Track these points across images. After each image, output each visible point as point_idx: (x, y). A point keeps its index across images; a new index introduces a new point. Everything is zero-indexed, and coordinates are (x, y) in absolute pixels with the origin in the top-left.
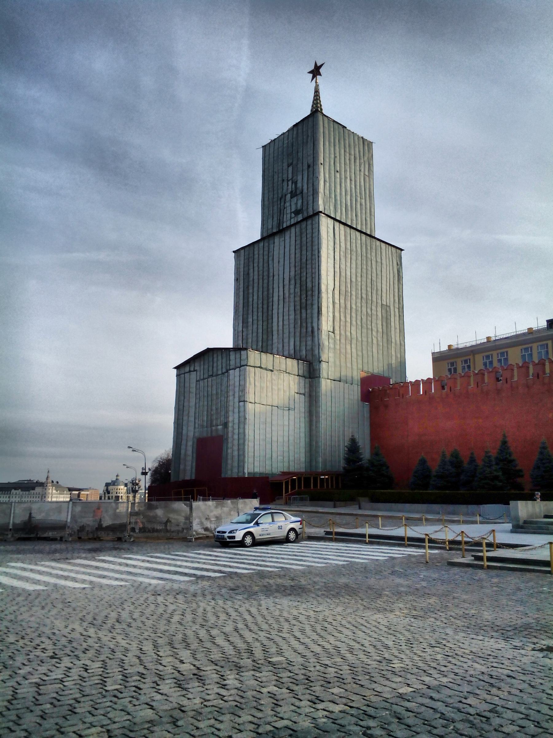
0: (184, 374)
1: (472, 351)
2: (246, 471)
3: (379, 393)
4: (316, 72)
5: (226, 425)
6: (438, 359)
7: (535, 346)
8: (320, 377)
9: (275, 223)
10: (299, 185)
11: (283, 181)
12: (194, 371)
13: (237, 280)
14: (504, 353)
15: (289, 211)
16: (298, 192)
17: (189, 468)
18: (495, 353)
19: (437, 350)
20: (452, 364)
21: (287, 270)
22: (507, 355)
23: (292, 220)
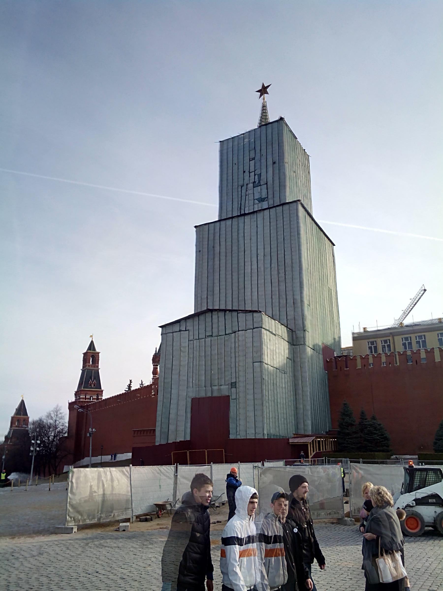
0: (173, 332)
1: (391, 333)
2: (265, 432)
3: (336, 363)
5: (233, 385)
6: (357, 338)
8: (305, 344)
9: (236, 205)
10: (263, 177)
11: (244, 172)
12: (186, 331)
13: (199, 252)
14: (422, 336)
15: (251, 197)
16: (262, 183)
17: (181, 428)
19: (356, 331)
20: (372, 343)
21: (261, 247)
22: (425, 338)
23: (256, 206)
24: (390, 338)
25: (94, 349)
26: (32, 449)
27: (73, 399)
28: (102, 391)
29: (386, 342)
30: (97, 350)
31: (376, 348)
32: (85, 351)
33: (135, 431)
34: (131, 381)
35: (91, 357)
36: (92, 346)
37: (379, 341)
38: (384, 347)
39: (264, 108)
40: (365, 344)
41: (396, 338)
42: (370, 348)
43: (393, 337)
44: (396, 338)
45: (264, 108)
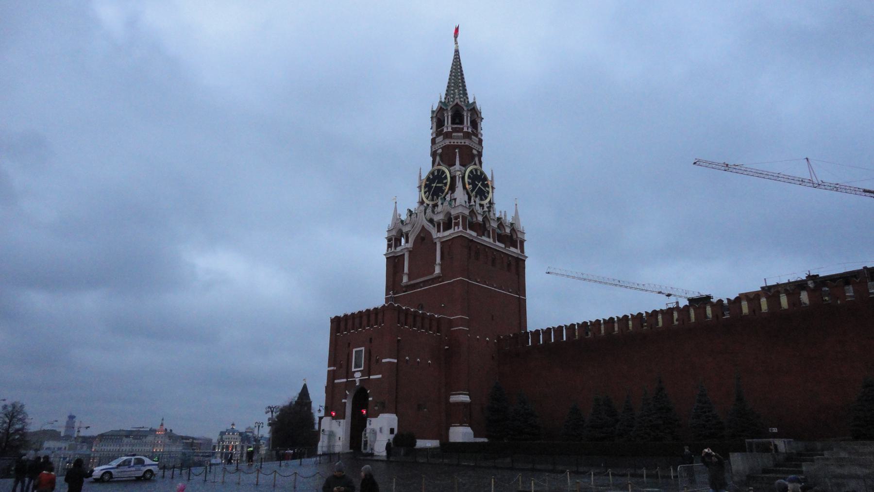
45: (457, 52)
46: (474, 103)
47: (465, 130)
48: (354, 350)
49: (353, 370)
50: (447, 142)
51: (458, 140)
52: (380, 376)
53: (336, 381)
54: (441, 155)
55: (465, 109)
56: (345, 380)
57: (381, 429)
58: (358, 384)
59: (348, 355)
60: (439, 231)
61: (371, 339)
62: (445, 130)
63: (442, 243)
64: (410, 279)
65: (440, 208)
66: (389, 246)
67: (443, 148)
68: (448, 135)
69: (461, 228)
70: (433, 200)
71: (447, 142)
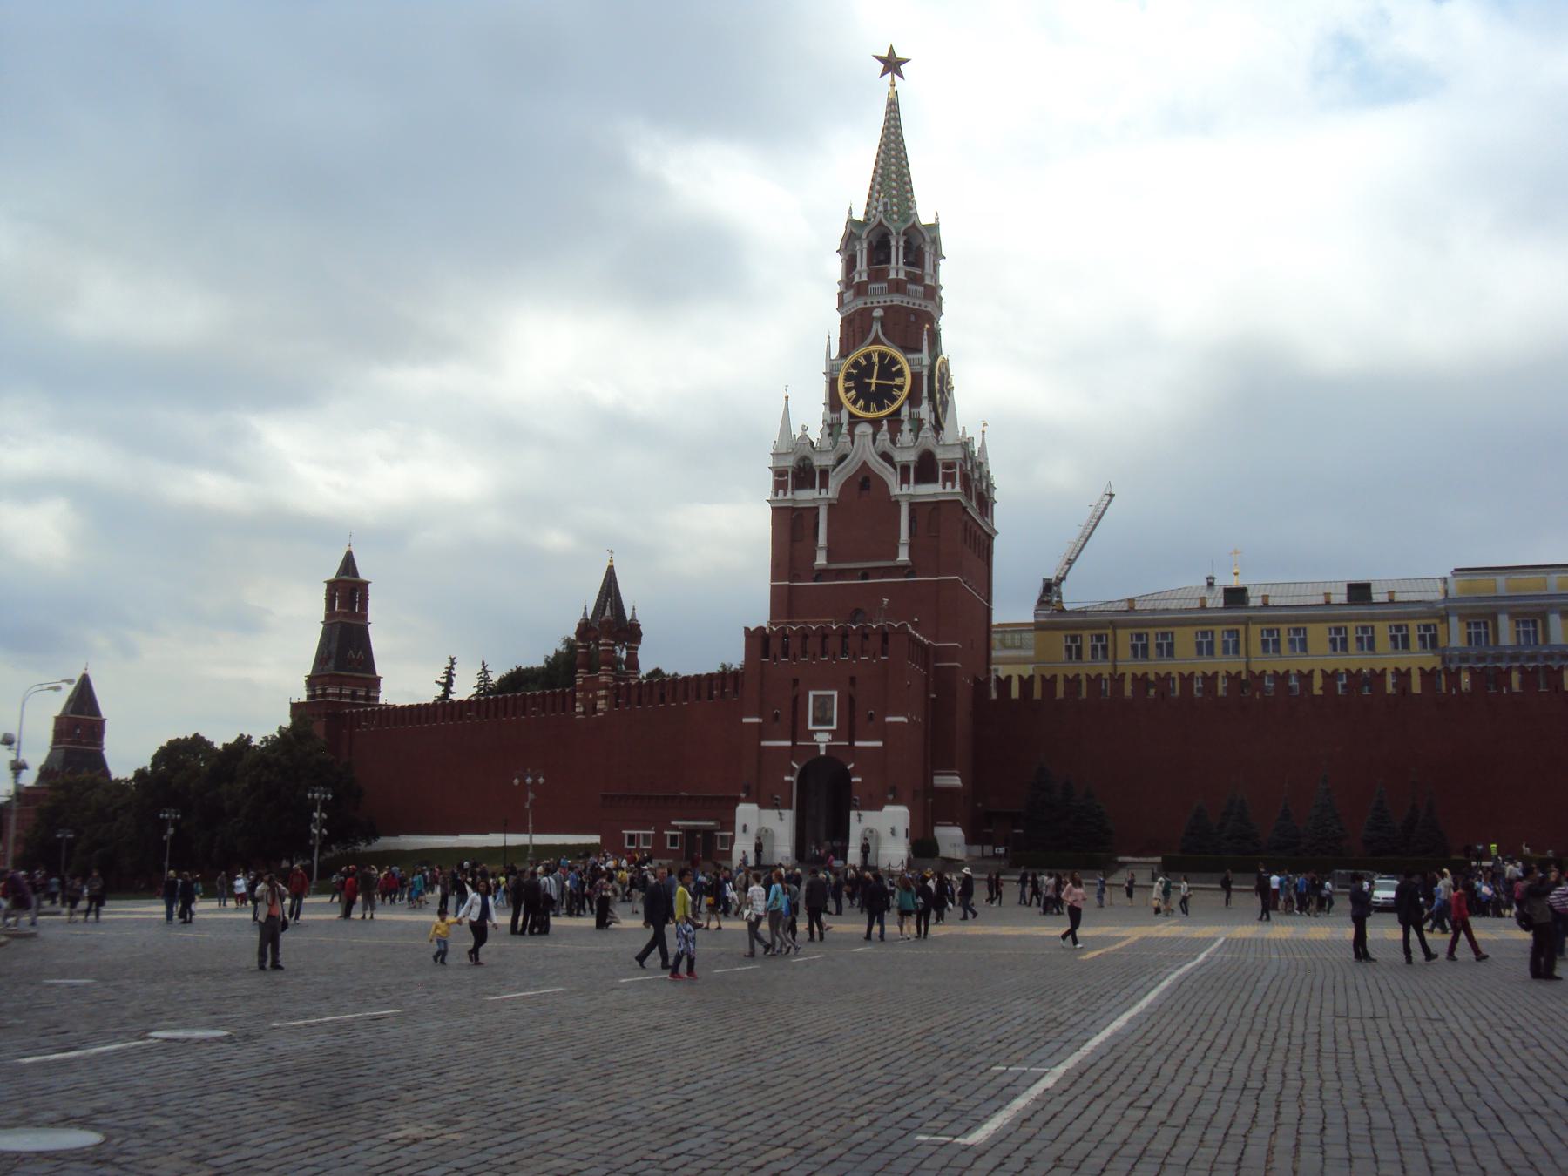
1: (1111, 622)
4: (892, 64)
7: (1218, 630)
18: (1152, 632)
20: (1074, 638)
24: (1109, 631)
25: (356, 574)
26: (316, 815)
27: (302, 695)
28: (378, 679)
29: (1099, 638)
30: (363, 576)
31: (1079, 649)
32: (332, 576)
33: (605, 797)
34: (452, 661)
35: (347, 594)
36: (349, 564)
37: (1086, 634)
38: (1094, 648)
39: (893, 107)
40: (1060, 640)
41: (1120, 632)
42: (1069, 649)
43: (1114, 629)
44: (1120, 632)
45: (893, 107)
46: (934, 228)
47: (928, 281)
48: (811, 694)
49: (811, 727)
50: (897, 299)
51: (912, 299)
52: (880, 744)
53: (764, 743)
54: (882, 320)
55: (928, 239)
56: (789, 743)
57: (893, 832)
58: (823, 753)
59: (795, 700)
60: (904, 480)
61: (853, 679)
62: (893, 275)
63: (911, 504)
64: (829, 559)
65: (906, 437)
66: (779, 485)
67: (886, 309)
68: (898, 287)
69: (958, 483)
70: (867, 408)
71: (897, 299)
